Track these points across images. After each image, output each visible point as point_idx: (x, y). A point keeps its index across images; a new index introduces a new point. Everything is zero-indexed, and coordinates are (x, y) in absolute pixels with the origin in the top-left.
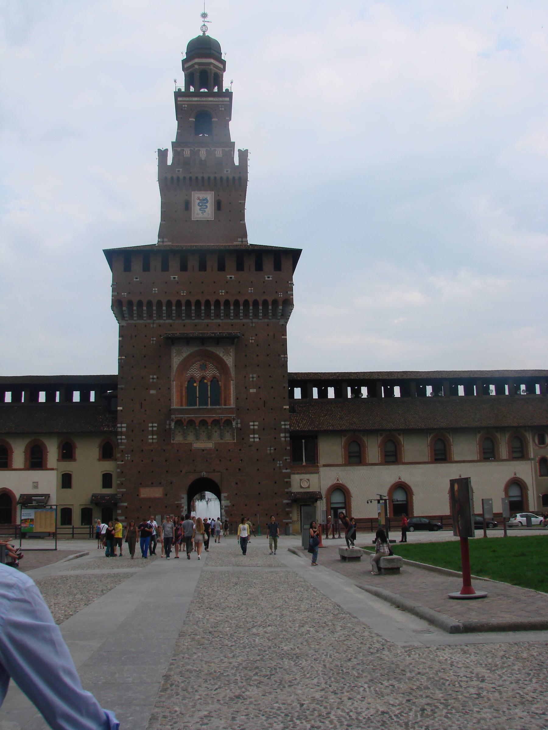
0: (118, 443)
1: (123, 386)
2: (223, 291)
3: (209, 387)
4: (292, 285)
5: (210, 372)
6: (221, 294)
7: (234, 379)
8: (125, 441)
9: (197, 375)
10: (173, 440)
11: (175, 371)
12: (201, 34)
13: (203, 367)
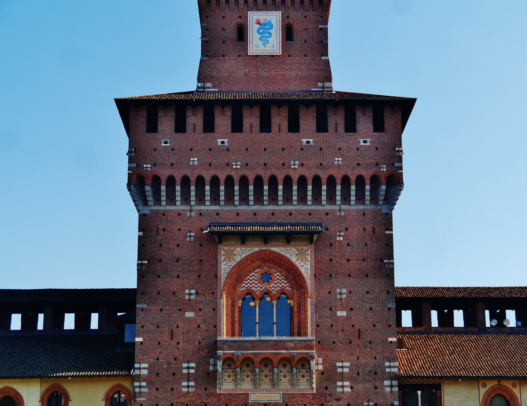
0: (135, 393)
1: (145, 306)
2: (297, 163)
3: (275, 307)
4: (400, 154)
5: (275, 284)
6: (293, 167)
8: (146, 390)
9: (256, 290)
10: (220, 389)
11: (222, 284)
13: (267, 278)
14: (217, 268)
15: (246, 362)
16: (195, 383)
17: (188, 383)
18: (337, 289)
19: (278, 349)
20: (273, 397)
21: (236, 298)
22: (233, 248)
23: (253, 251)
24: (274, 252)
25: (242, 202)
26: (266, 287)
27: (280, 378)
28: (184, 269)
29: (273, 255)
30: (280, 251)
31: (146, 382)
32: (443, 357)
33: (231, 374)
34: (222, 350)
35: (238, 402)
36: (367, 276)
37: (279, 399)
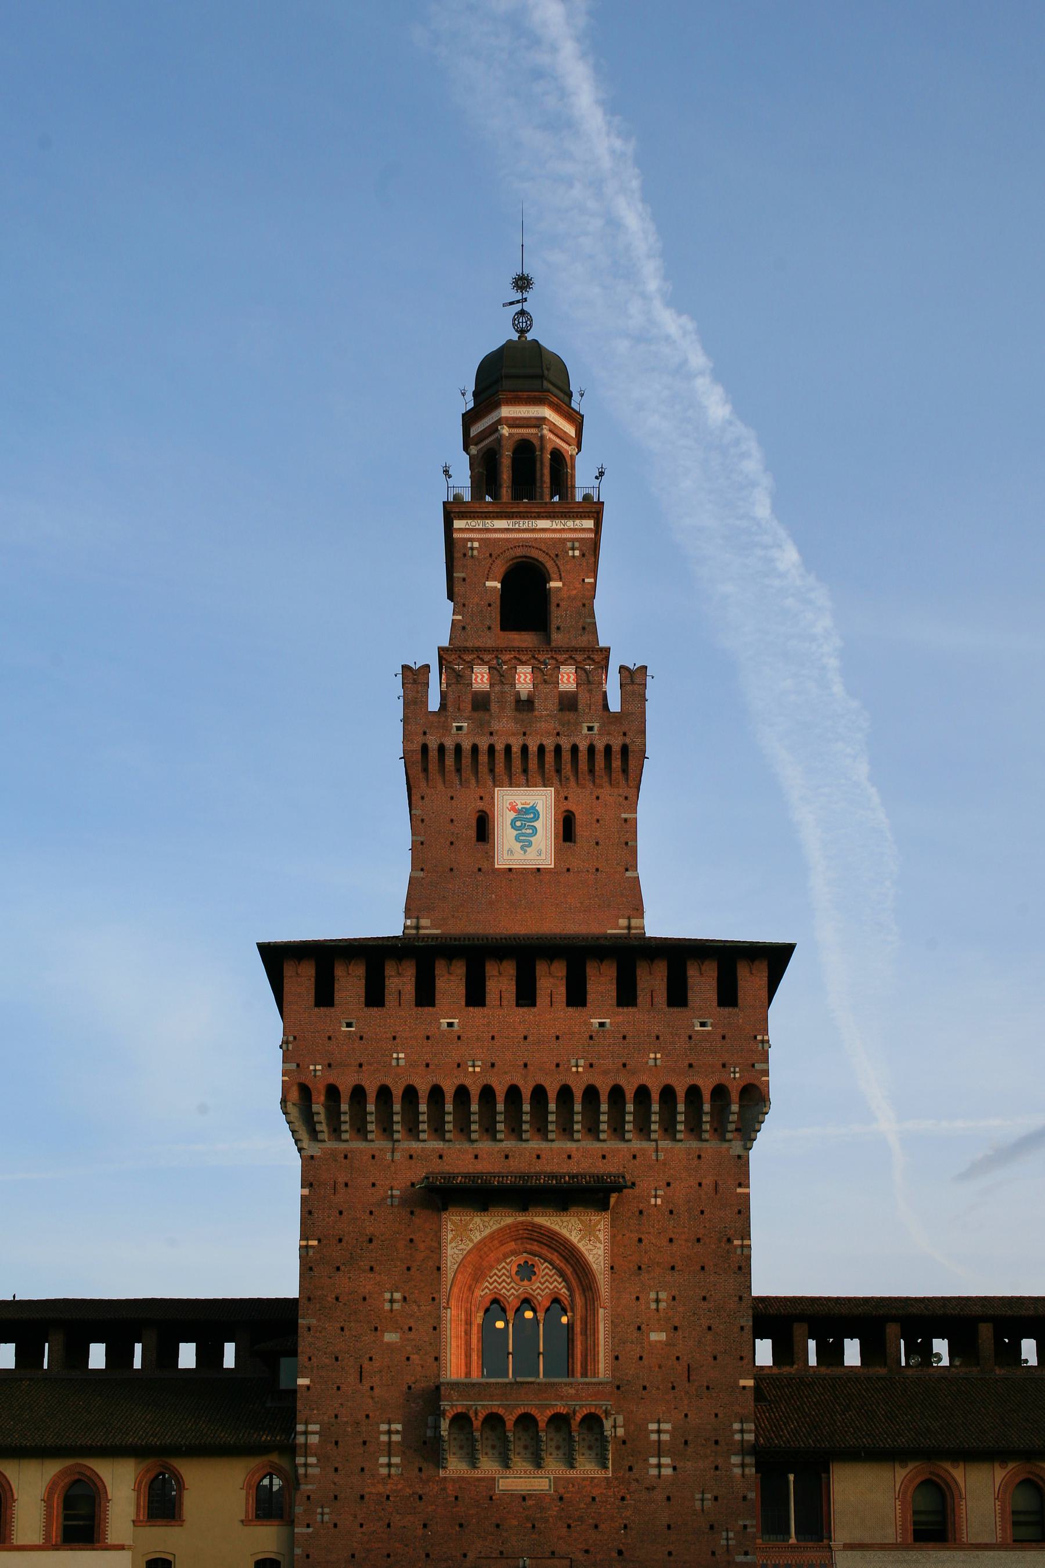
12: (515, 336)
14: (440, 1254)
18: (651, 1293)
22: (468, 1218)
23: (503, 1223)
24: (541, 1226)
25: (485, 1134)
30: (551, 1224)
31: (316, 1456)
32: (832, 1416)
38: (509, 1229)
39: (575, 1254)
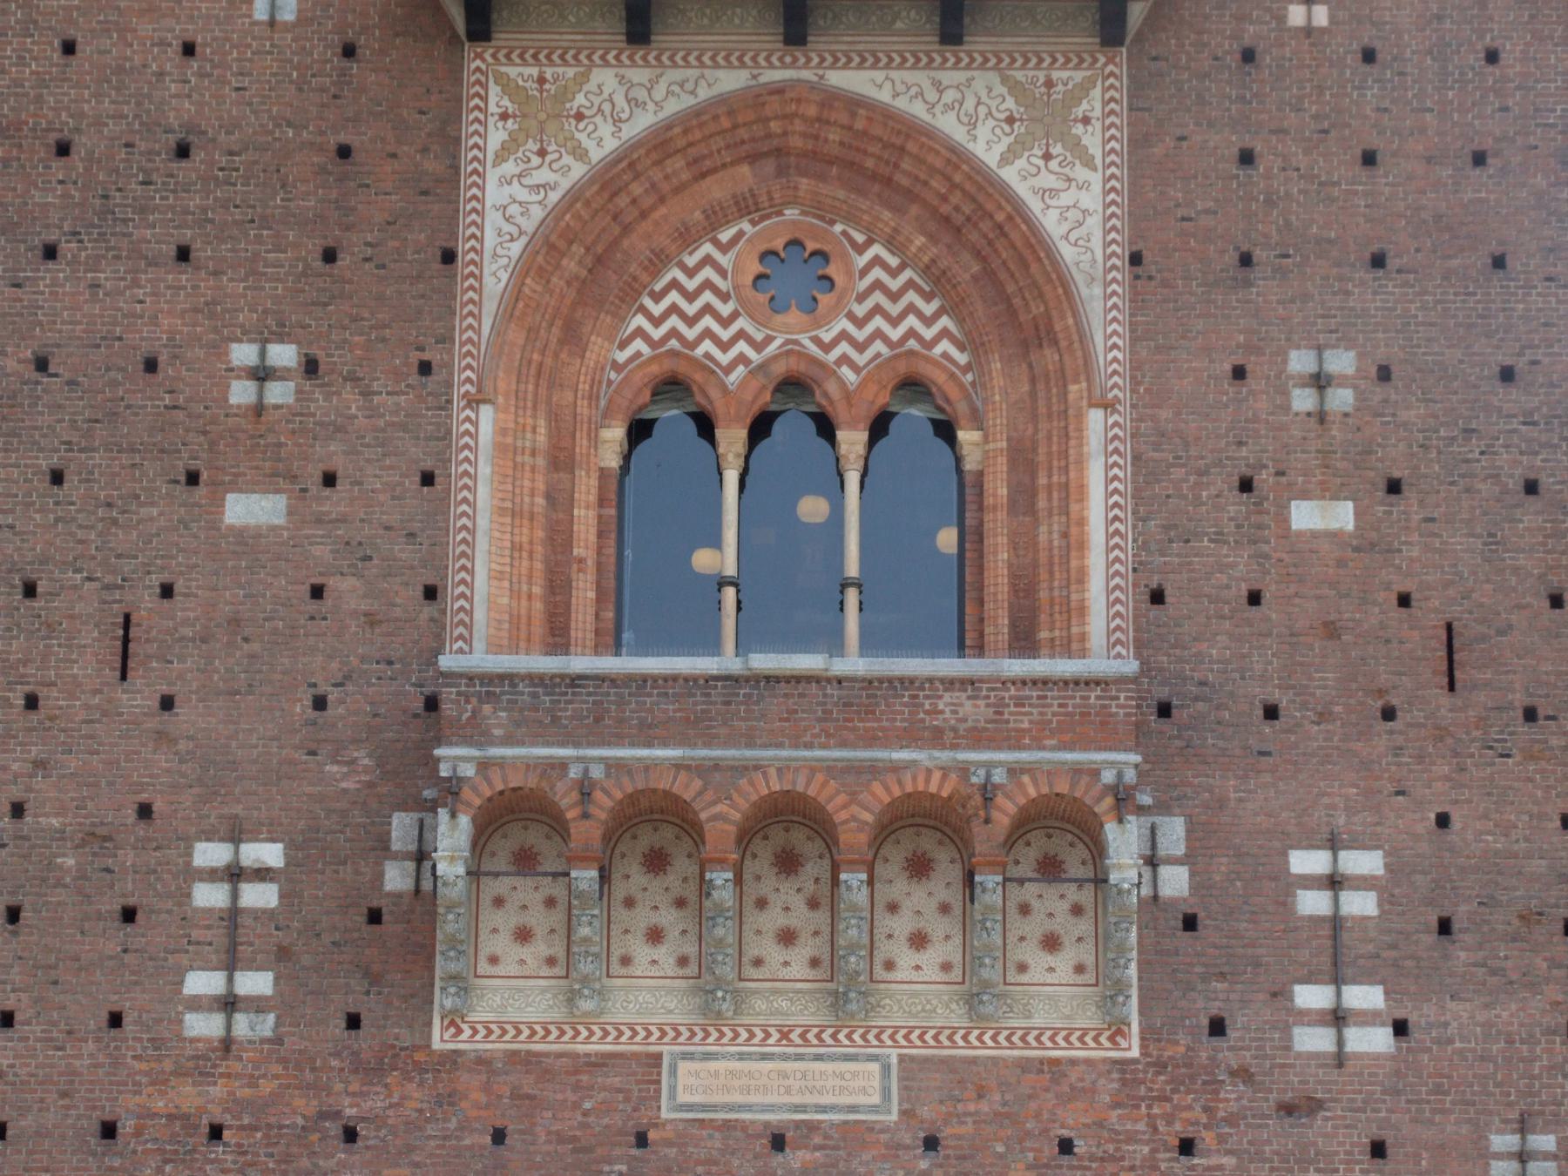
5: (860, 323)
7: (1120, 388)
9: (725, 359)
15: (647, 838)
16: (277, 980)
17: (230, 980)
19: (871, 741)
20: (830, 1083)
21: (583, 408)
22: (571, 72)
23: (704, 93)
24: (855, 103)
26: (796, 342)
27: (884, 950)
28: (225, 204)
29: (844, 118)
30: (896, 95)
33: (538, 919)
34: (467, 741)
35: (585, 1114)
36: (1499, 262)
37: (875, 1099)
38: (731, 113)
39: (990, 207)
